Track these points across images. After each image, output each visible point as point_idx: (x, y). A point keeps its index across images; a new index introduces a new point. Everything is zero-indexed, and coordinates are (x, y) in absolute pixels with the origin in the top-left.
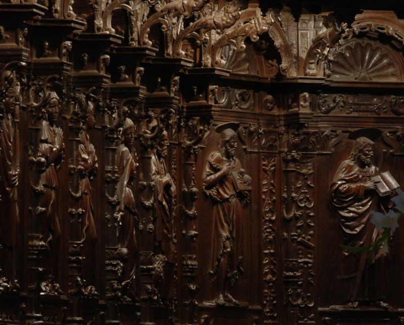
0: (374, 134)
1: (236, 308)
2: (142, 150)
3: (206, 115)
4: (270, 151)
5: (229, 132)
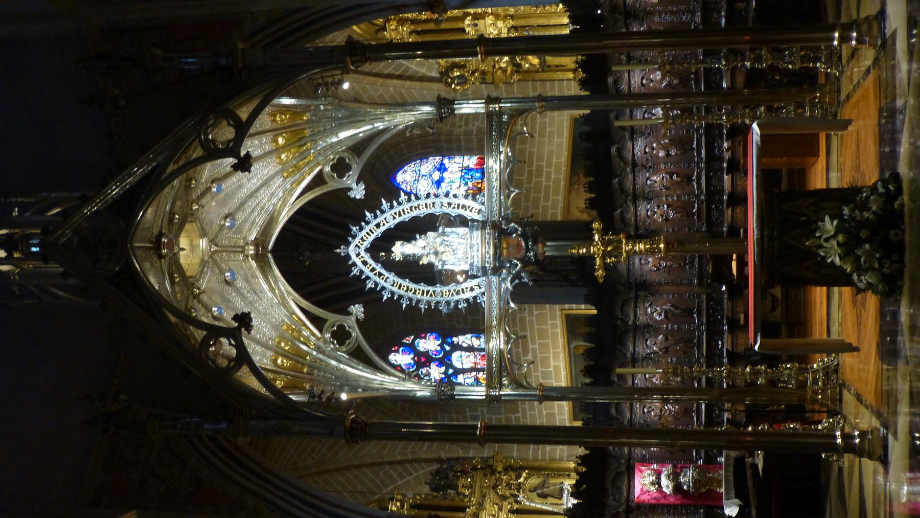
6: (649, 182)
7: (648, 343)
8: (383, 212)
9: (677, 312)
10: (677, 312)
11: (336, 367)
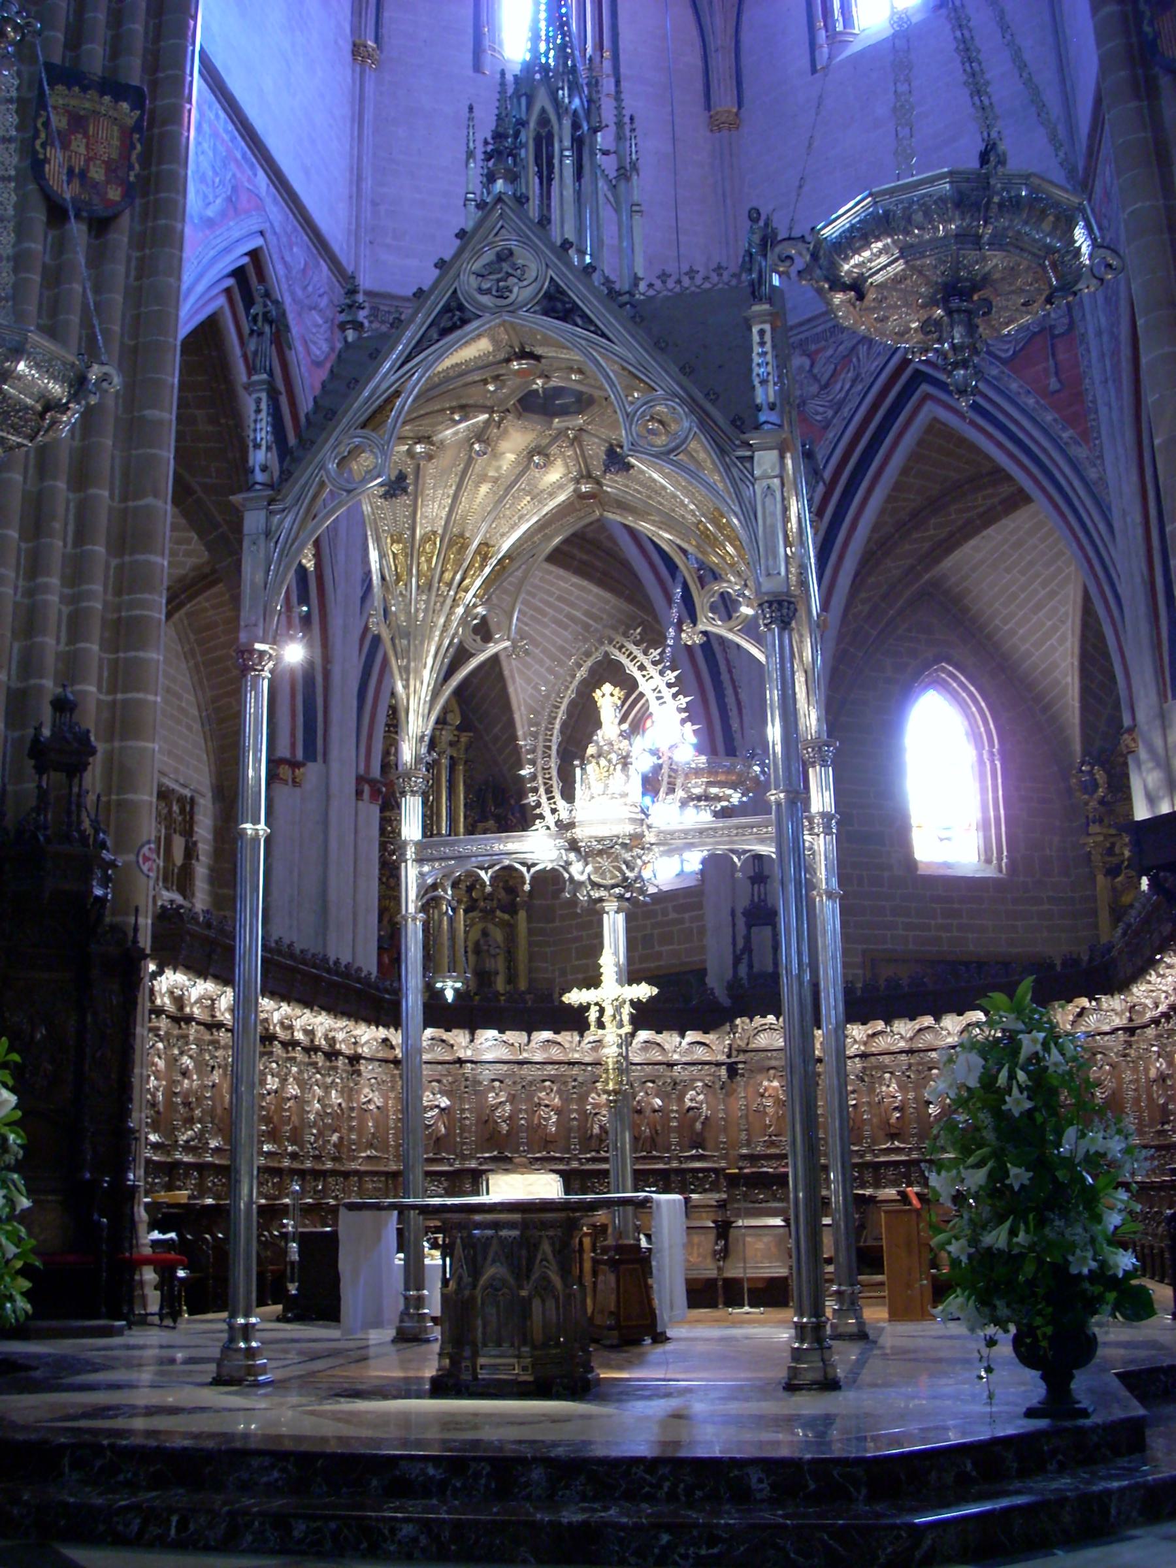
0: (439, 1081)
1: (376, 1157)
2: (327, 1088)
3: (359, 1073)
4: (393, 1088)
5: (373, 1081)
6: (887, 1076)
7: (650, 1085)
8: (662, 673)
9: (698, 1126)
10: (698, 1126)
11: (435, 626)
